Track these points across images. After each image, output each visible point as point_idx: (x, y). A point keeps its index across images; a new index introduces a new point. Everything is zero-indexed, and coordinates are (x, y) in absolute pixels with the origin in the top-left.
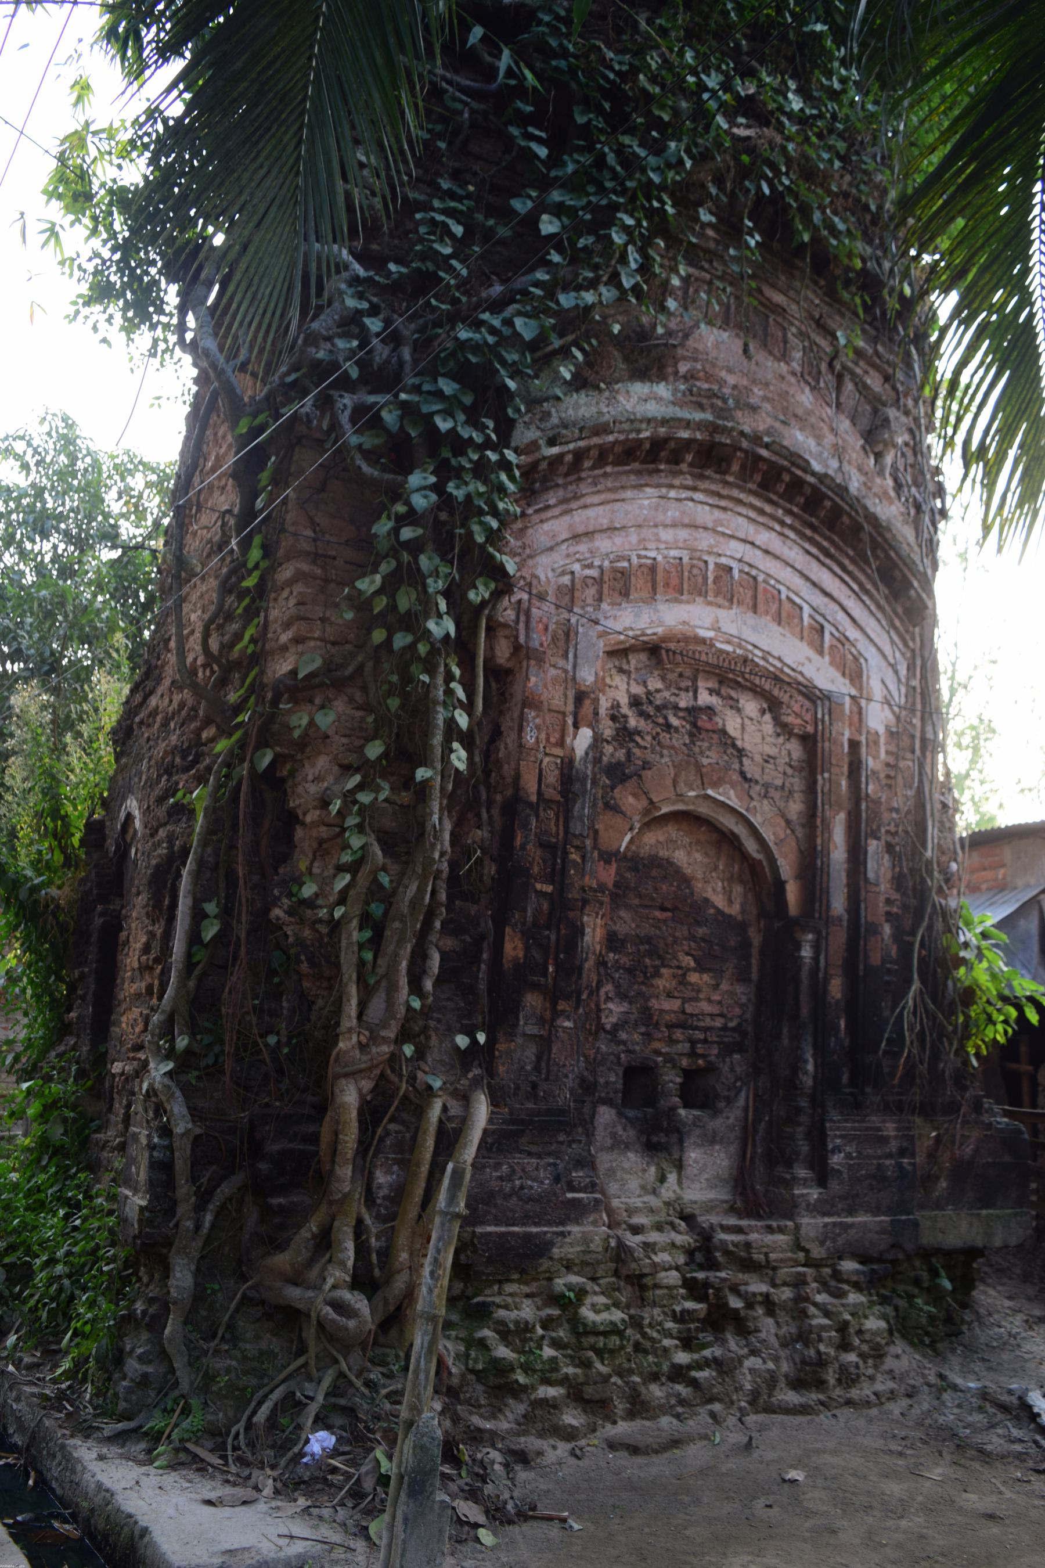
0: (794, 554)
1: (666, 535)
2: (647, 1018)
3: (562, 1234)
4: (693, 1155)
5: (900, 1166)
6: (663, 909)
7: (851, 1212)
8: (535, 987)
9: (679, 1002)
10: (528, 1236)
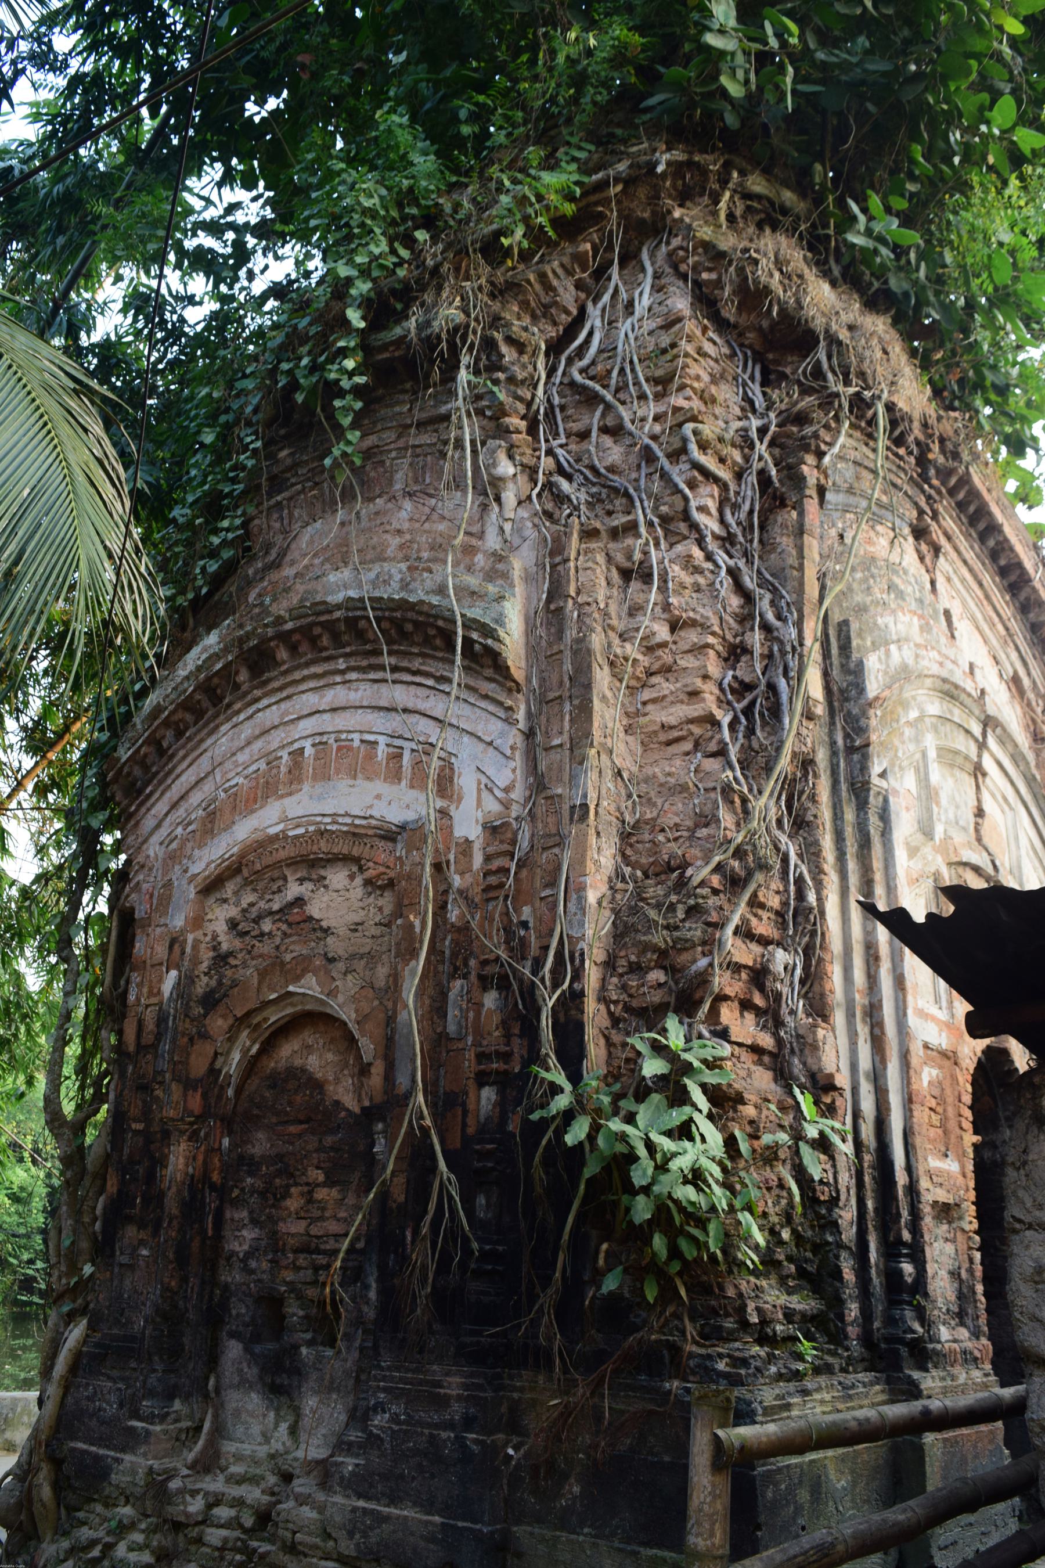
0: (362, 692)
1: (241, 758)
2: (275, 1244)
3: (118, 1461)
4: (310, 1403)
5: (460, 1440)
6: (301, 1122)
7: (393, 1501)
8: (129, 1219)
9: (303, 1224)
10: (97, 1458)
